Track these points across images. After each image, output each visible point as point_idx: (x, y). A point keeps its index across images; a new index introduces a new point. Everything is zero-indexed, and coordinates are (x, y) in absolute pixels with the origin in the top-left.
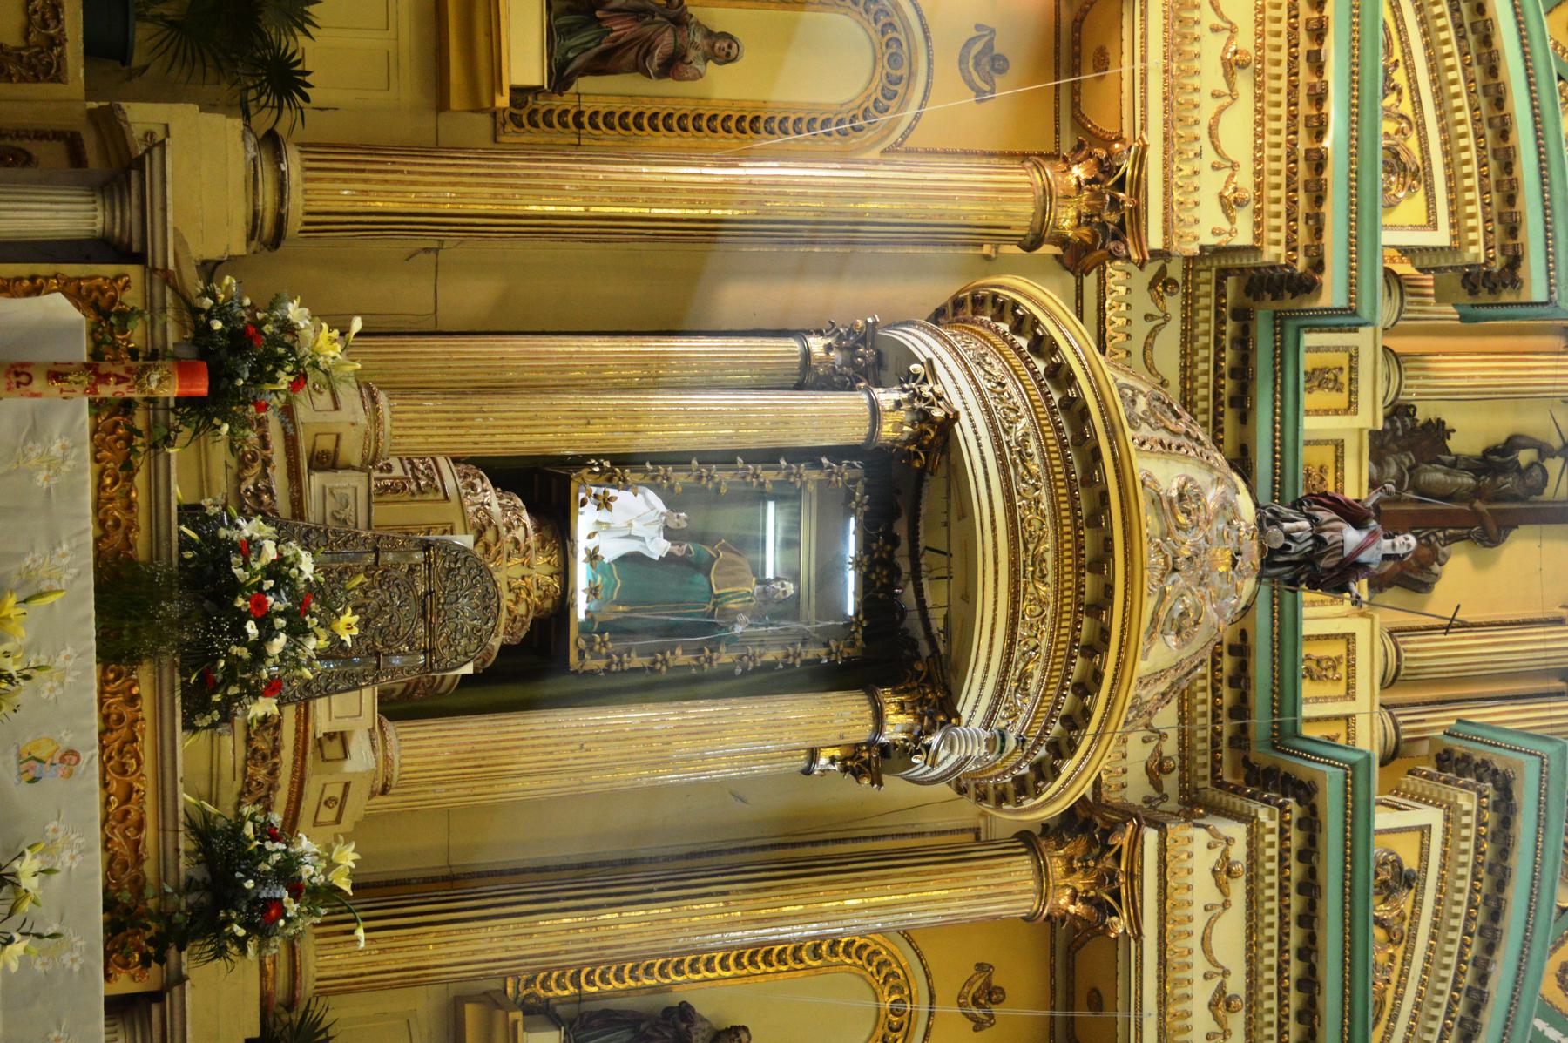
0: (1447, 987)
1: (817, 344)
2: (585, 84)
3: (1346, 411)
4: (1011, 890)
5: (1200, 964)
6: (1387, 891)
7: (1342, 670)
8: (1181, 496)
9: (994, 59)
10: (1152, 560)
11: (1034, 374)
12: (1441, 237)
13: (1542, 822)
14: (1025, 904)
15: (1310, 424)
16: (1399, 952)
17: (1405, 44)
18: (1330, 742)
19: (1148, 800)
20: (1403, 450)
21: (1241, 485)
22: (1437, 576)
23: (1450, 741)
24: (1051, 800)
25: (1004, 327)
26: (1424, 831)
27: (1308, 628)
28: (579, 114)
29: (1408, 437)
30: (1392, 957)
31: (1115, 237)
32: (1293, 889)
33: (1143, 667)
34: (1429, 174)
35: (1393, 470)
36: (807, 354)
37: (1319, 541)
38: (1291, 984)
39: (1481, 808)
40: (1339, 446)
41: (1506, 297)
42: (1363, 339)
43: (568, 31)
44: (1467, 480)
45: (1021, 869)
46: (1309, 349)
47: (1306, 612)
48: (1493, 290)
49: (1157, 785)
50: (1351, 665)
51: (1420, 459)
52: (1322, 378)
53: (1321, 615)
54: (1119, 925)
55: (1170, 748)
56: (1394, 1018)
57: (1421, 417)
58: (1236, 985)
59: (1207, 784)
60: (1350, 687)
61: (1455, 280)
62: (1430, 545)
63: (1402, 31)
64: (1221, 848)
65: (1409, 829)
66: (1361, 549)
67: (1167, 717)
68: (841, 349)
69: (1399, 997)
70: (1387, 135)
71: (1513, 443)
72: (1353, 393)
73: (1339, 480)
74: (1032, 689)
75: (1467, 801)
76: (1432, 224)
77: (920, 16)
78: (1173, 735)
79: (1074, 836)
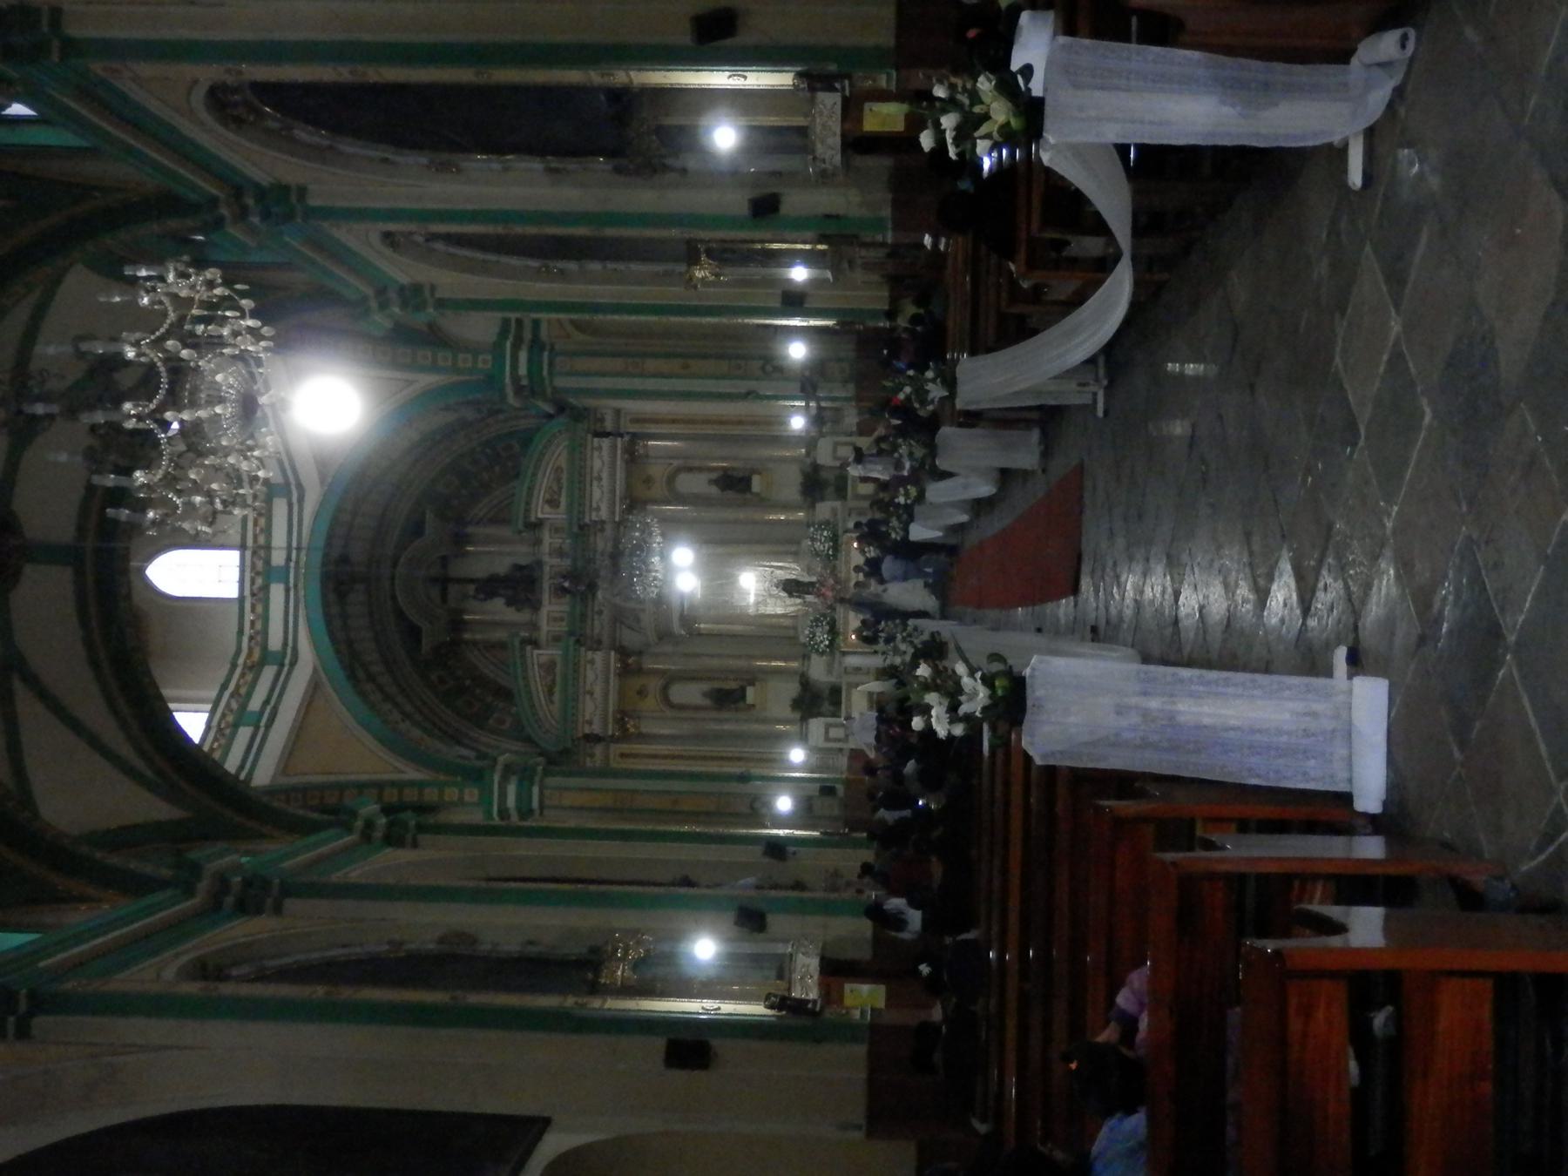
58: (595, 483)
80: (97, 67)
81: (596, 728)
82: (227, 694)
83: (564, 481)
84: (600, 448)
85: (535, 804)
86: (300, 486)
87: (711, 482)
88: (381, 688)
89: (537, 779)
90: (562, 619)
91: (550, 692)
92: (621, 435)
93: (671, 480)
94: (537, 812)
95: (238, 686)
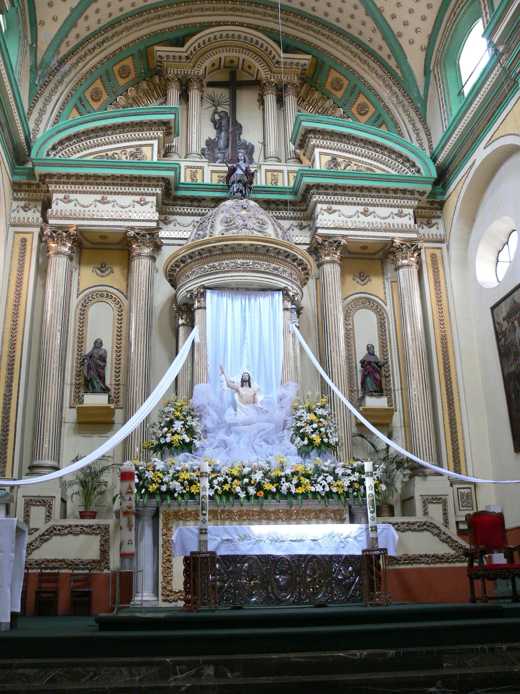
0: (364, 150)
1: (181, 322)
2: (108, 383)
3: (203, 170)
4: (332, 271)
6: (337, 165)
7: (275, 173)
8: (226, 222)
9: (102, 267)
10: (244, 232)
11: (191, 262)
12: (155, 143)
13: (320, 122)
14: (337, 268)
15: (207, 181)
16: (354, 162)
17: (101, 152)
18: (296, 178)
19: (310, 230)
20: (214, 152)
21: (224, 203)
22: (250, 143)
23: (296, 144)
24: (308, 261)
25: (178, 270)
26: (321, 154)
27: (264, 184)
28: (115, 384)
29: (210, 150)
30: (355, 165)
31: (153, 236)
32: (335, 192)
33: (273, 236)
34: (137, 146)
35: (219, 155)
36: (183, 325)
37: (239, 181)
38: (361, 194)
39: (315, 138)
40: (212, 172)
41: (172, 125)
42: (183, 164)
43: (93, 387)
44: (223, 134)
45: (327, 268)
46: (185, 180)
47: (259, 184)
48: (171, 128)
49: (305, 227)
50: (274, 171)
51: (217, 147)
52: (193, 176)
53: (260, 180)
54: (343, 242)
55: (295, 223)
56: (372, 165)
57: (205, 147)
59: (305, 213)
60: (280, 171)
61: (167, 138)
62: (241, 145)
63: (97, 152)
64: (323, 211)
65: (320, 158)
66: (242, 169)
67: (286, 224)
68: (182, 315)
69: (366, 163)
70: (127, 158)
71: (213, 121)
72: (198, 167)
73: (222, 172)
74: (278, 266)
75: (313, 142)
76: (152, 145)
77: (90, 288)
78: (292, 222)
79: (319, 253)
81: (58, 206)
84: (400, 215)
87: (370, 349)
90: (193, 180)
93: (368, 303)
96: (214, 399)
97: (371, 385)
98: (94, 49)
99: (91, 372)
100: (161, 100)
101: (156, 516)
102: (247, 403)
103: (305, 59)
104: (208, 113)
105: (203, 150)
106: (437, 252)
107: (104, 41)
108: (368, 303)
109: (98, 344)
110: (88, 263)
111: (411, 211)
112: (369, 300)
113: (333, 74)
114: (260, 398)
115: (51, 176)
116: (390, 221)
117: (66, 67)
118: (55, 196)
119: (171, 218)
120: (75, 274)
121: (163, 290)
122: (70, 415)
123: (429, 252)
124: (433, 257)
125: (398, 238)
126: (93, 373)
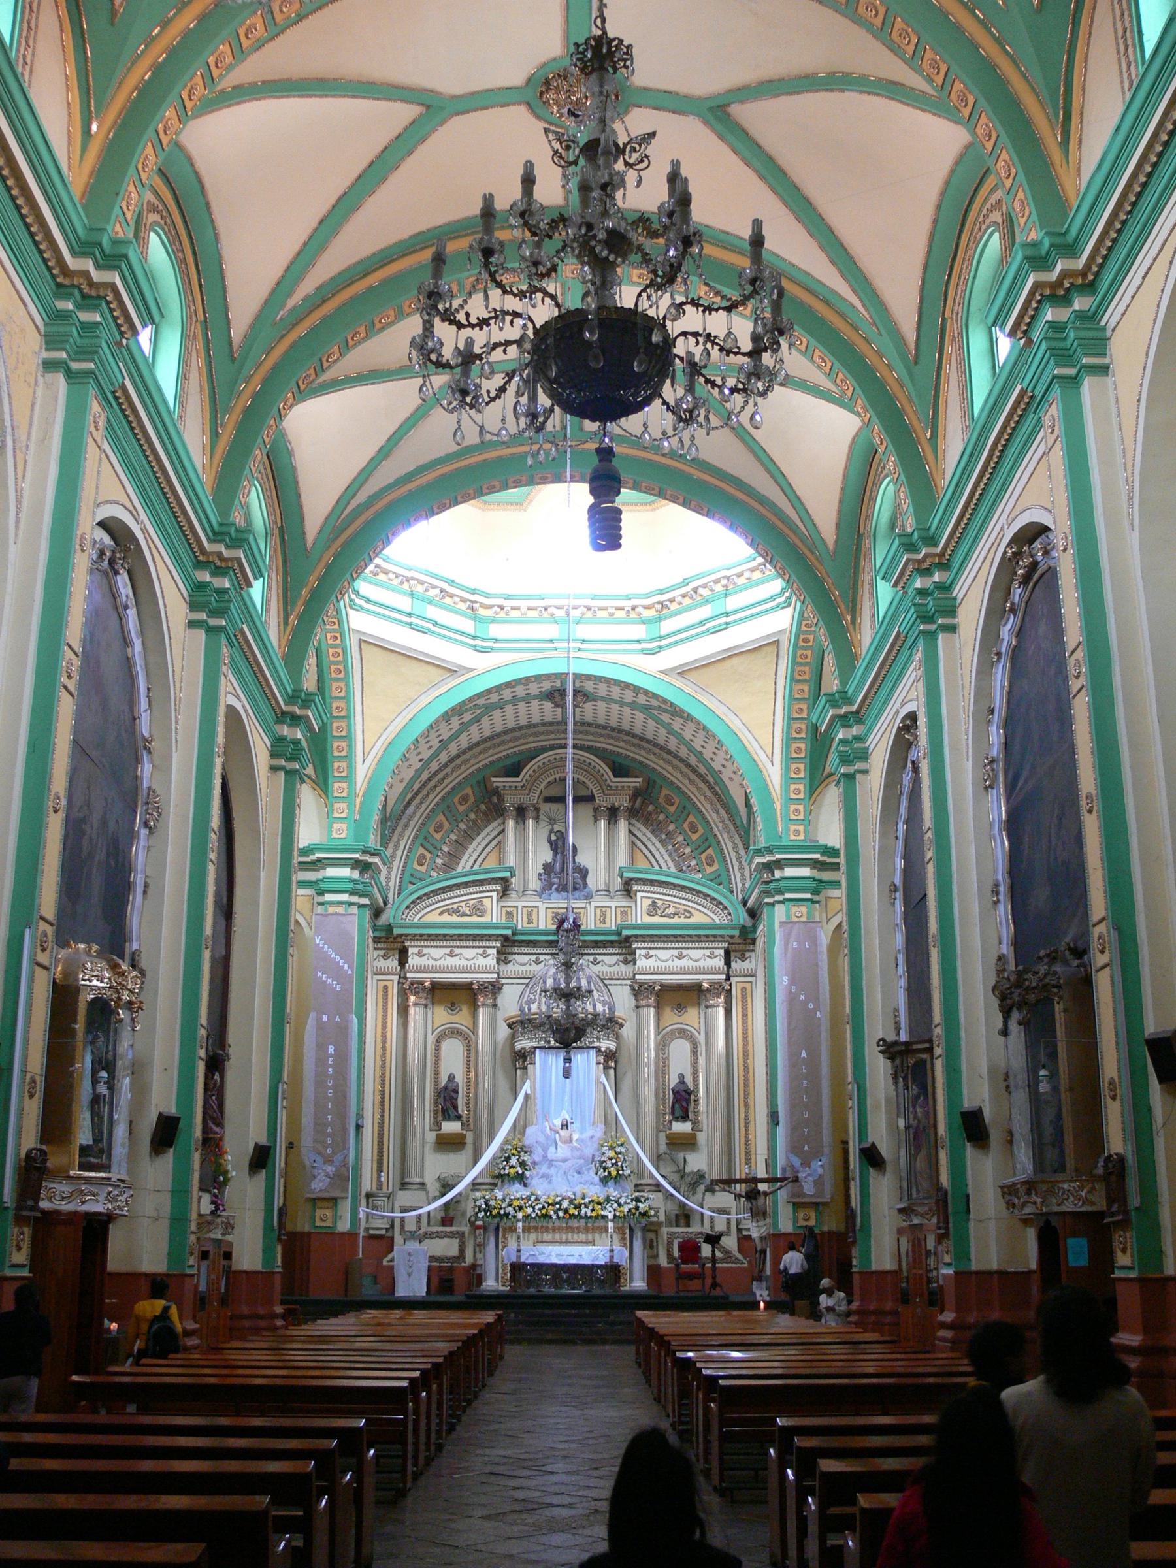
5: (670, 963)
12: (494, 894)
55: (621, 958)
71: (550, 841)
80: (1053, 412)
81: (413, 961)
82: (445, 586)
83: (676, 920)
85: (328, 897)
86: (660, 649)
87: (681, 1077)
88: (455, 737)
89: (355, 899)
91: (452, 912)
92: (728, 978)
93: (683, 1033)
94: (320, 899)
95: (451, 596)
96: (542, 1139)
97: (678, 1112)
98: (435, 787)
99: (447, 1102)
100: (500, 821)
101: (497, 1229)
102: (565, 1142)
103: (635, 782)
104: (545, 832)
105: (540, 874)
106: (748, 986)
107: (444, 778)
108: (683, 1033)
109: (451, 1078)
110: (440, 1002)
111: (722, 952)
112: (684, 1031)
113: (665, 791)
114: (575, 1137)
115: (407, 935)
116: (701, 963)
117: (411, 809)
118: (411, 950)
119: (511, 957)
120: (430, 1012)
121: (503, 1032)
122: (431, 1137)
123: (740, 986)
124: (744, 990)
125: (705, 980)
126: (448, 1105)
